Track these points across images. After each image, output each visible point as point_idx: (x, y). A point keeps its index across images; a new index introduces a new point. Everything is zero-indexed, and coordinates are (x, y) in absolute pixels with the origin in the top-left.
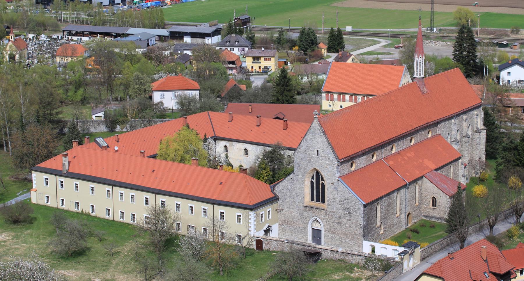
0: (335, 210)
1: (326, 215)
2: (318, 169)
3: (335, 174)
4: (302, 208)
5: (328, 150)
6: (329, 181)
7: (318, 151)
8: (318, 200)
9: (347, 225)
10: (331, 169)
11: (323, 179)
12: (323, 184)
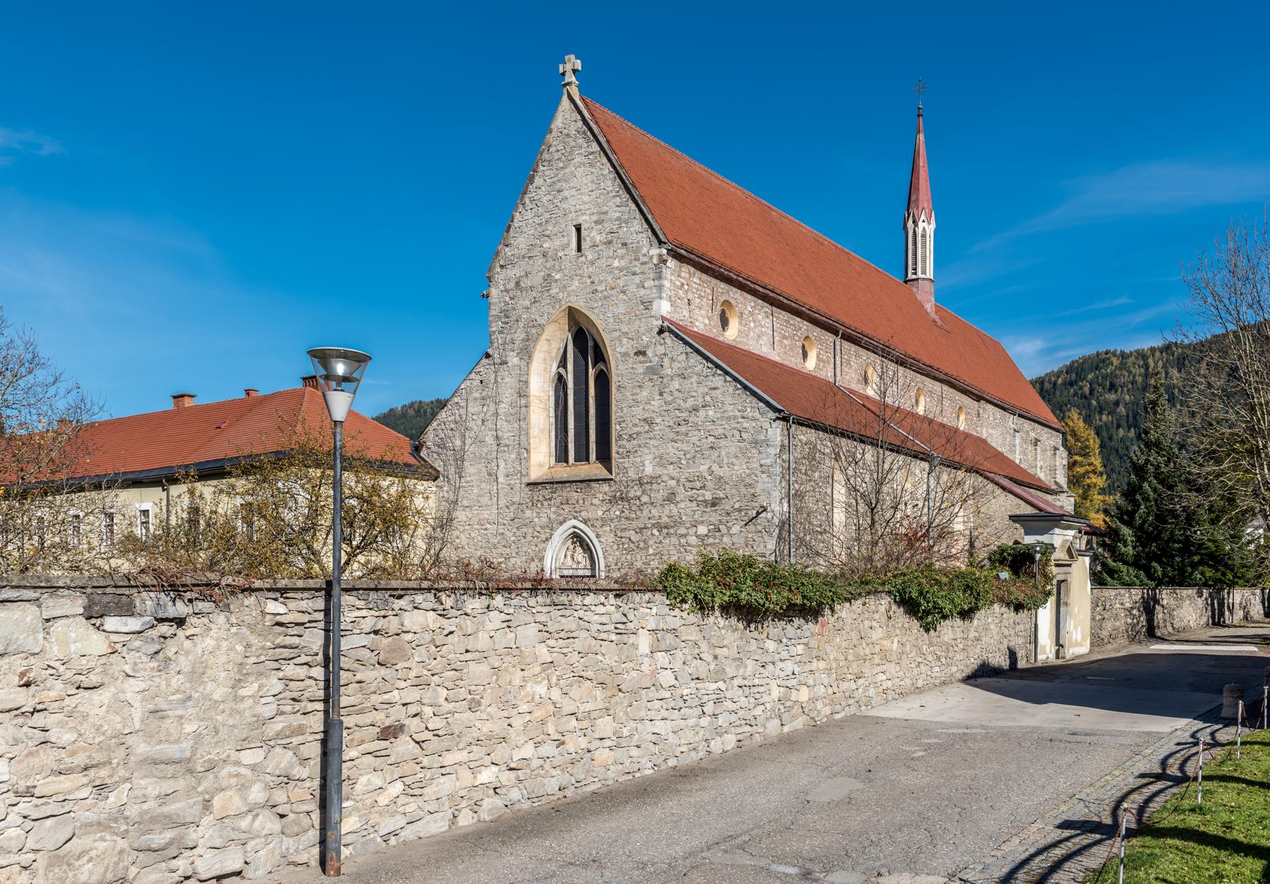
0: (649, 470)
1: (613, 500)
2: (580, 305)
3: (647, 304)
4: (521, 494)
5: (617, 206)
6: (627, 346)
7: (578, 229)
8: (582, 456)
9: (702, 530)
10: (632, 288)
11: (600, 357)
12: (603, 381)
